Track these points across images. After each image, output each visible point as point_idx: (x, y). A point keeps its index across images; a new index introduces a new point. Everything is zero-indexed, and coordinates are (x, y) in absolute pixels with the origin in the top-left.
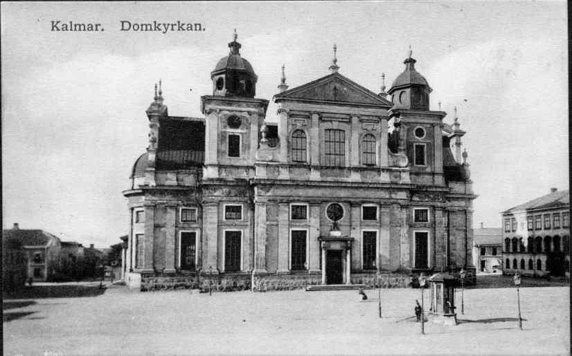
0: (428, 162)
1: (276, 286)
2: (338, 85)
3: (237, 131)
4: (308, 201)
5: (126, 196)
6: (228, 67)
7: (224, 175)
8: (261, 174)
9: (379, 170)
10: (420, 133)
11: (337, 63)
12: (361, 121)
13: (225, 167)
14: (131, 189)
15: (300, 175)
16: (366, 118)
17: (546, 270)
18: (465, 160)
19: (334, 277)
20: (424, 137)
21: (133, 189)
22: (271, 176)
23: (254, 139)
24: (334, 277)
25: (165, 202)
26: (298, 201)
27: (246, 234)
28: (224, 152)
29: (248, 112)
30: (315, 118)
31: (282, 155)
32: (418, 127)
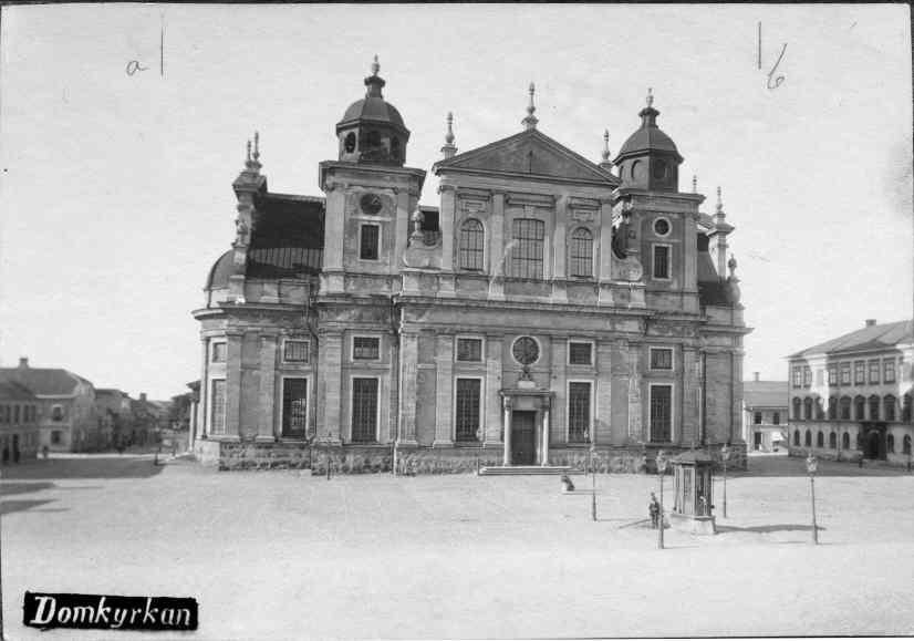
1: (432, 466)
4: (485, 333)
5: (199, 318)
6: (365, 117)
7: (352, 288)
8: (411, 287)
9: (596, 286)
10: (662, 227)
11: (535, 114)
13: (355, 275)
14: (205, 307)
17: (858, 449)
18: (732, 271)
20: (667, 234)
21: (209, 308)
22: (427, 292)
24: (523, 455)
25: (259, 329)
27: (385, 382)
29: (393, 189)
30: (499, 199)
32: (660, 218)
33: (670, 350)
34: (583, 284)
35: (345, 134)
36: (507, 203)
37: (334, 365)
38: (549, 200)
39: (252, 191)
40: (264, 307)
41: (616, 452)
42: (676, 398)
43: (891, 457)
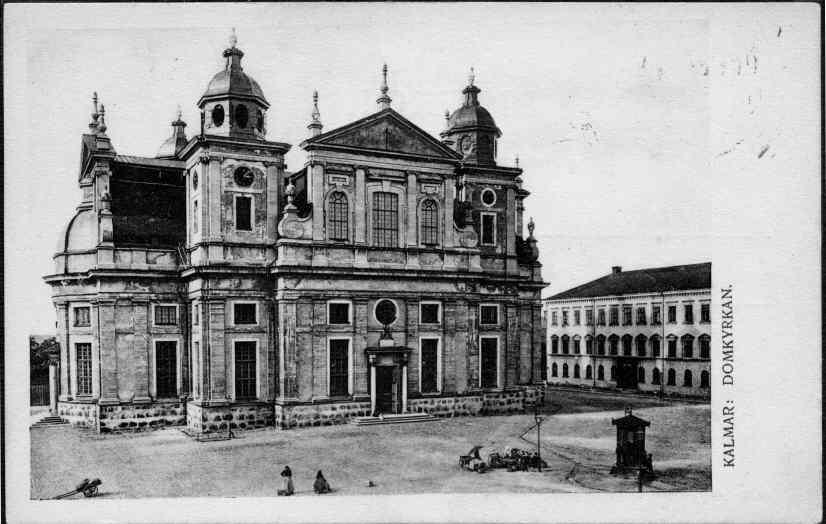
0: (498, 240)
1: (313, 421)
2: (391, 127)
3: (249, 191)
4: (351, 298)
7: (230, 258)
8: (287, 258)
10: (488, 198)
11: (388, 94)
12: (419, 181)
13: (234, 246)
15: (341, 259)
18: (531, 234)
19: (385, 405)
20: (494, 203)
21: (66, 273)
22: (307, 262)
23: (272, 203)
24: (385, 405)
25: (131, 295)
26: (339, 297)
27: (261, 342)
28: (229, 223)
29: (264, 162)
30: (361, 174)
31: (312, 229)
32: (488, 189)
33: (496, 307)
34: (430, 252)
35: (211, 106)
36: (368, 178)
37: (218, 330)
38: (402, 175)
39: (96, 156)
40: (134, 275)
41: (460, 399)
42: (501, 347)
43: (643, 387)
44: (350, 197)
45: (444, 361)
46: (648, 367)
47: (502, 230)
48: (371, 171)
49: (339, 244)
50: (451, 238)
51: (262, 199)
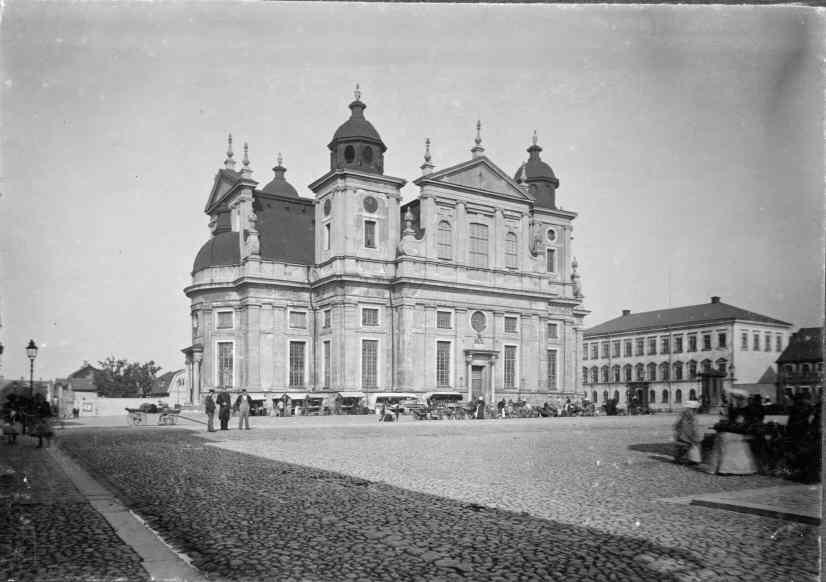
3: (374, 216)
11: (482, 145)
16: (509, 213)
30: (461, 207)
31: (428, 248)
35: (343, 147)
43: (652, 406)
44: (454, 224)
45: (521, 365)
46: (658, 389)
47: (562, 264)
48: (469, 205)
49: (444, 263)
50: (527, 264)
51: (385, 222)
